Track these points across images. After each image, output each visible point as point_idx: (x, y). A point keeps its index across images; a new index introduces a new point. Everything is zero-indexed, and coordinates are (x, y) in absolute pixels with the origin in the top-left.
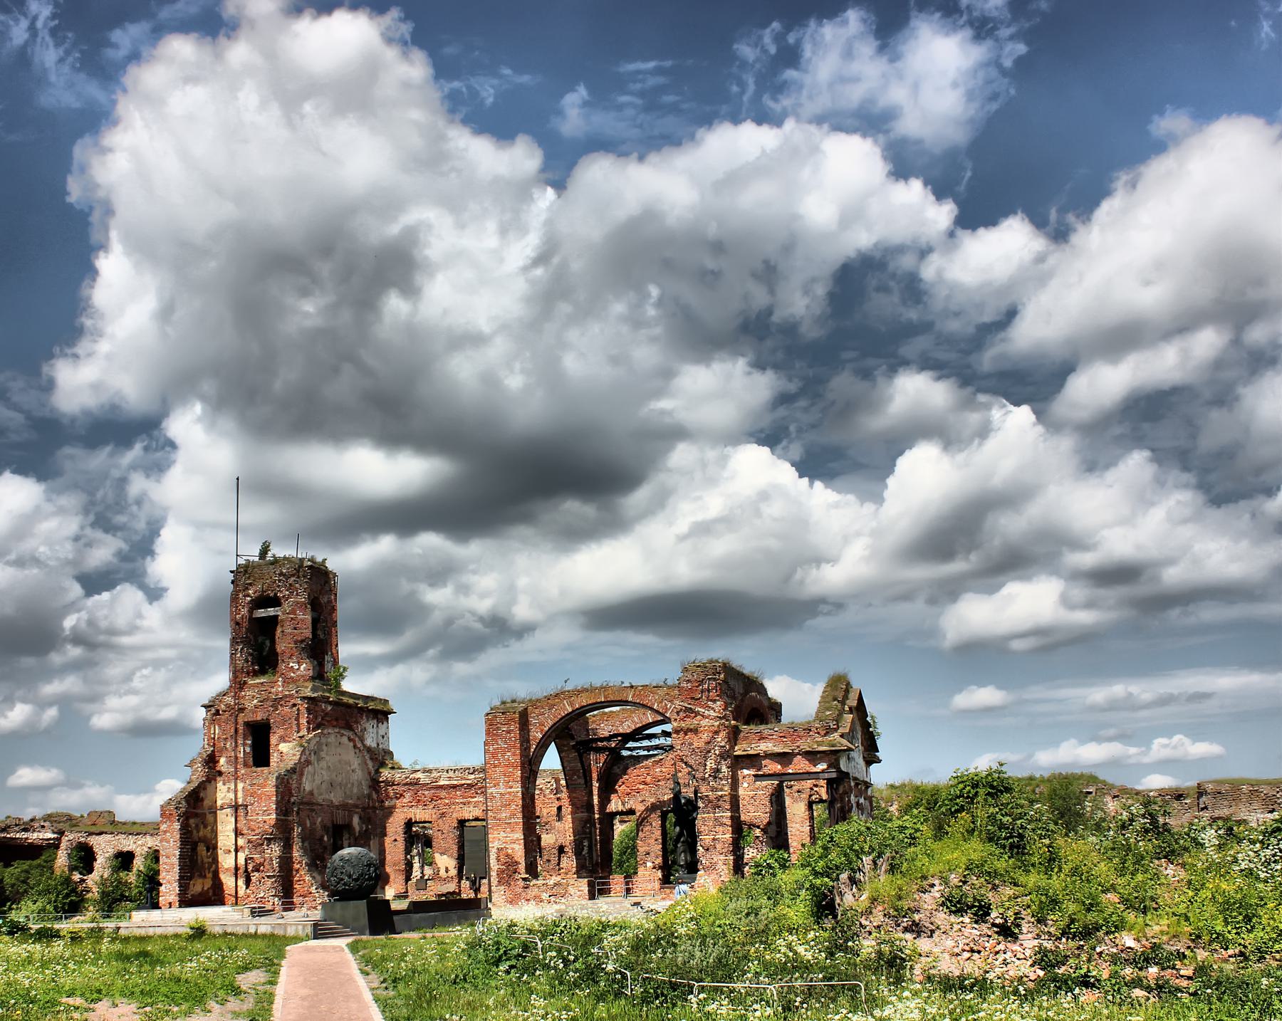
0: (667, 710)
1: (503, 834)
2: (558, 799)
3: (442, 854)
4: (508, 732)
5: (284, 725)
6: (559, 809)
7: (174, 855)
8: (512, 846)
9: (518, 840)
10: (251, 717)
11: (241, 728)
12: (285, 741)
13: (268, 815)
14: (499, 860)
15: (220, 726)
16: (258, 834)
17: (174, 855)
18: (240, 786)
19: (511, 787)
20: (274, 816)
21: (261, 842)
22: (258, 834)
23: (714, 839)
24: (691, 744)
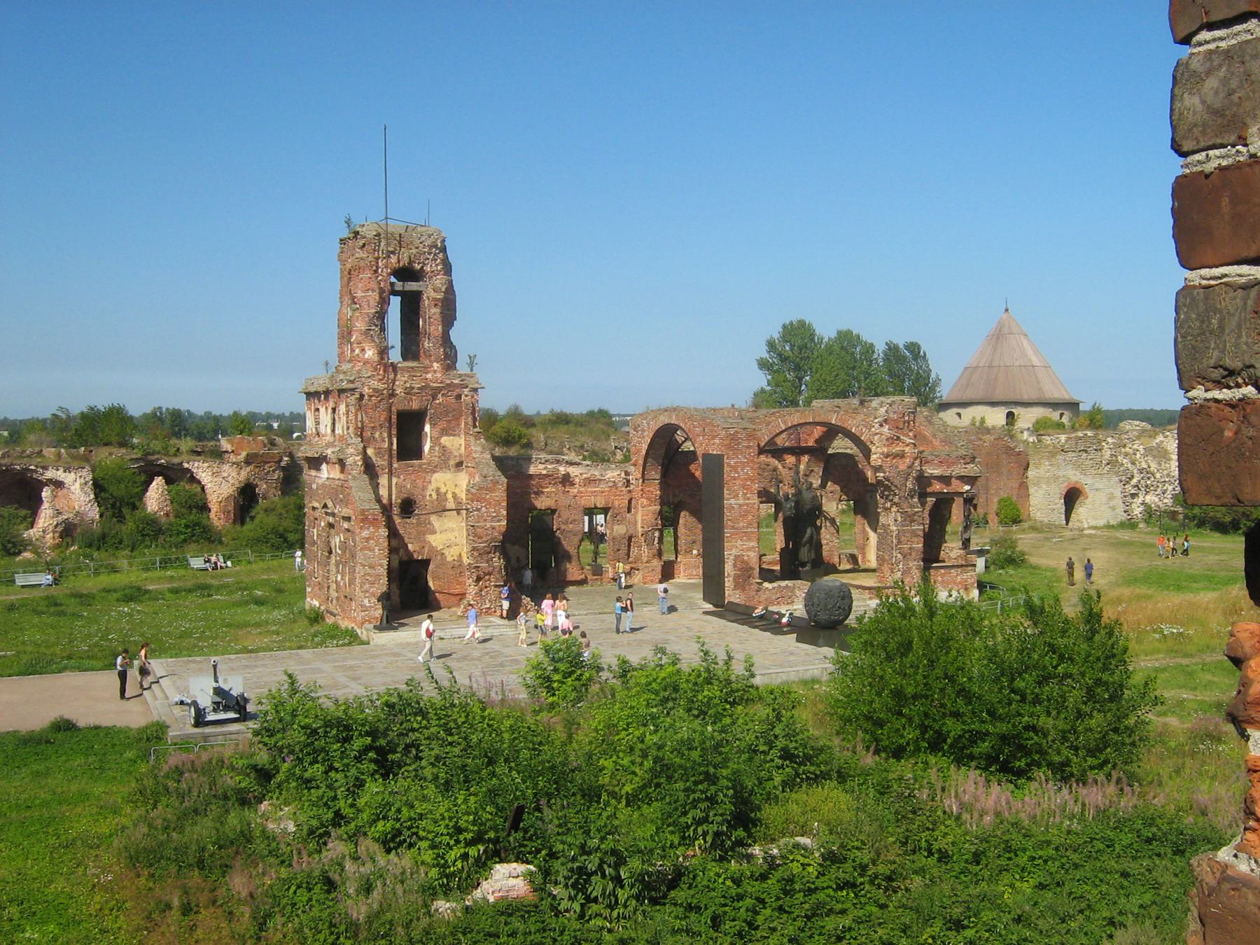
0: (862, 434)
1: (740, 542)
2: (630, 491)
3: (514, 544)
4: (748, 447)
5: (447, 415)
6: (630, 502)
7: (381, 566)
8: (749, 553)
9: (753, 547)
10: (403, 406)
11: (394, 417)
12: (447, 435)
13: (499, 521)
14: (735, 566)
15: (366, 413)
16: (486, 542)
17: (381, 566)
18: (394, 480)
19: (749, 499)
20: (504, 523)
21: (489, 550)
22: (486, 542)
23: (910, 548)
24: (897, 467)
